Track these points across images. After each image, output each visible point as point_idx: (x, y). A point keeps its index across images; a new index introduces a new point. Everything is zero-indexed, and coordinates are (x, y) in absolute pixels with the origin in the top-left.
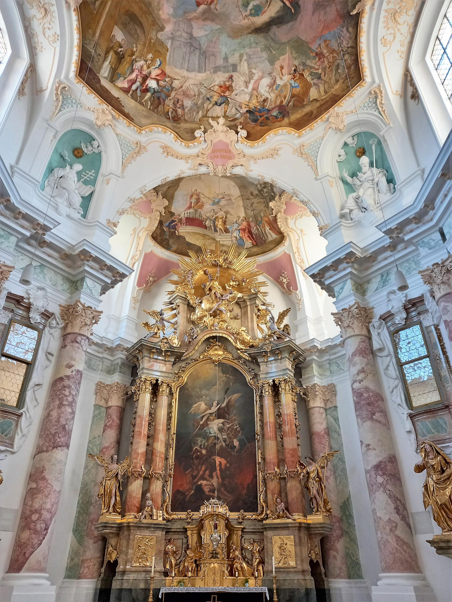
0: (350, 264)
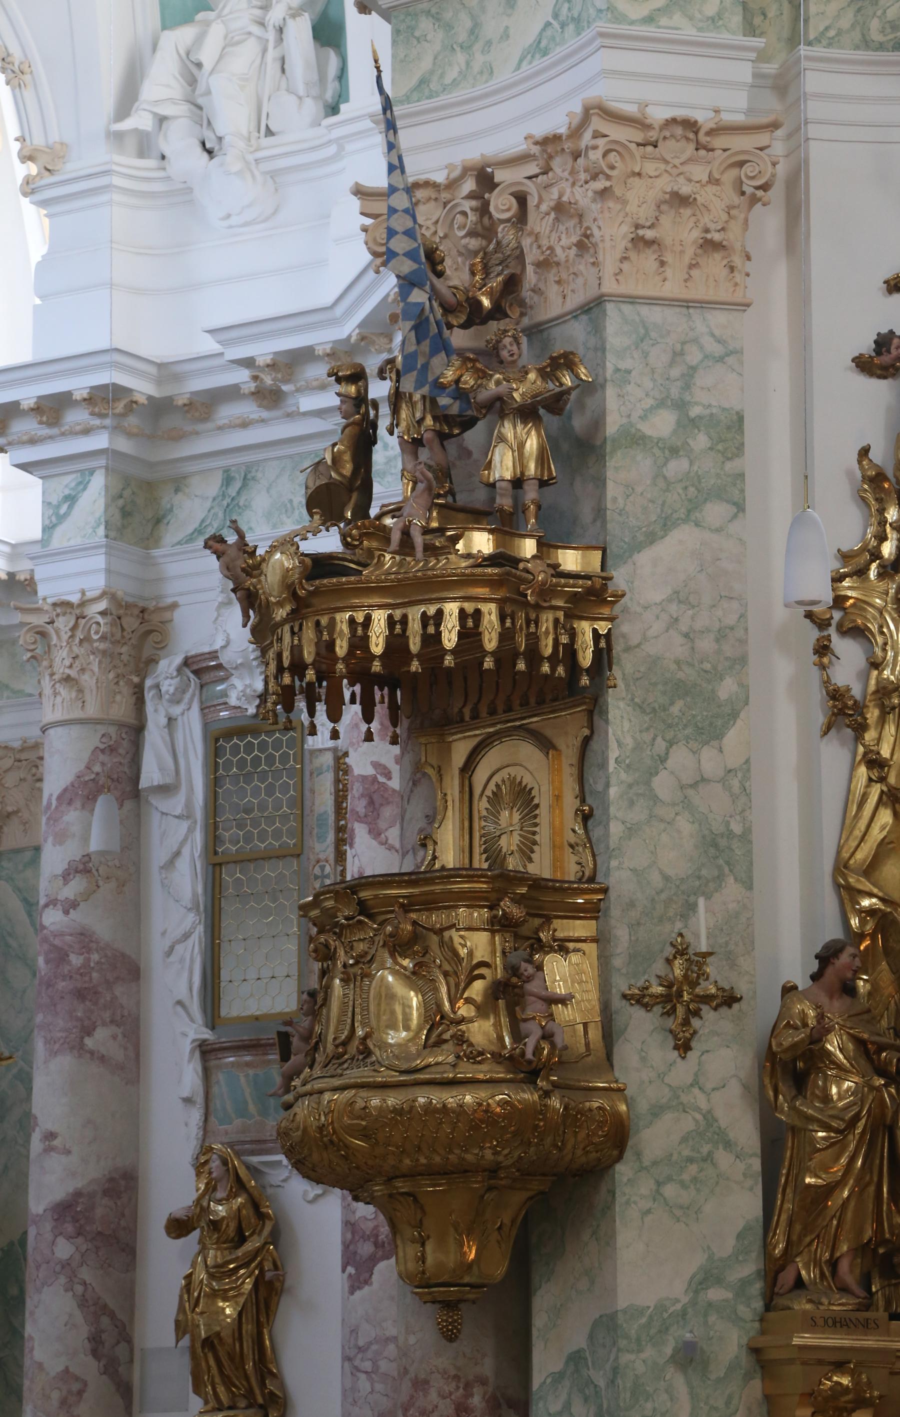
0: (108, 422)
